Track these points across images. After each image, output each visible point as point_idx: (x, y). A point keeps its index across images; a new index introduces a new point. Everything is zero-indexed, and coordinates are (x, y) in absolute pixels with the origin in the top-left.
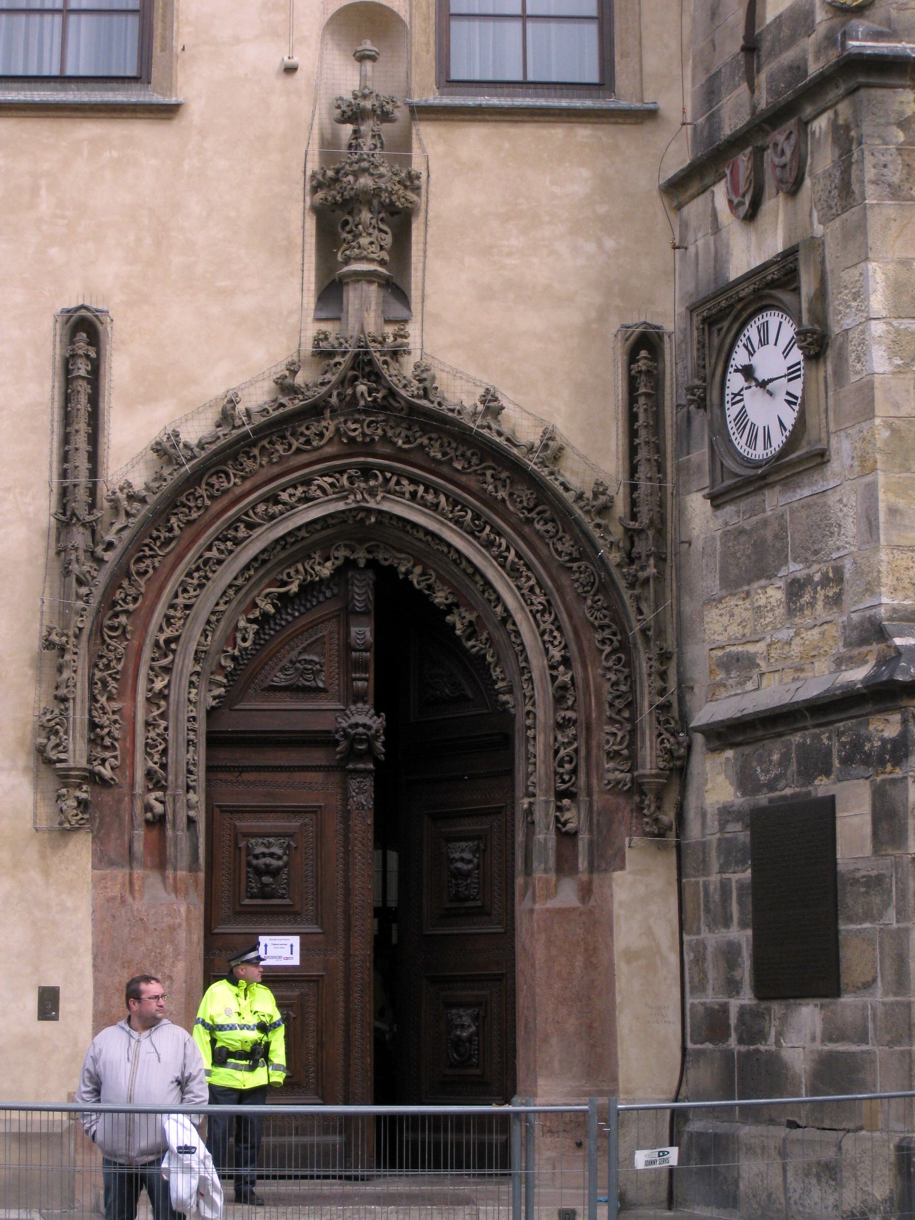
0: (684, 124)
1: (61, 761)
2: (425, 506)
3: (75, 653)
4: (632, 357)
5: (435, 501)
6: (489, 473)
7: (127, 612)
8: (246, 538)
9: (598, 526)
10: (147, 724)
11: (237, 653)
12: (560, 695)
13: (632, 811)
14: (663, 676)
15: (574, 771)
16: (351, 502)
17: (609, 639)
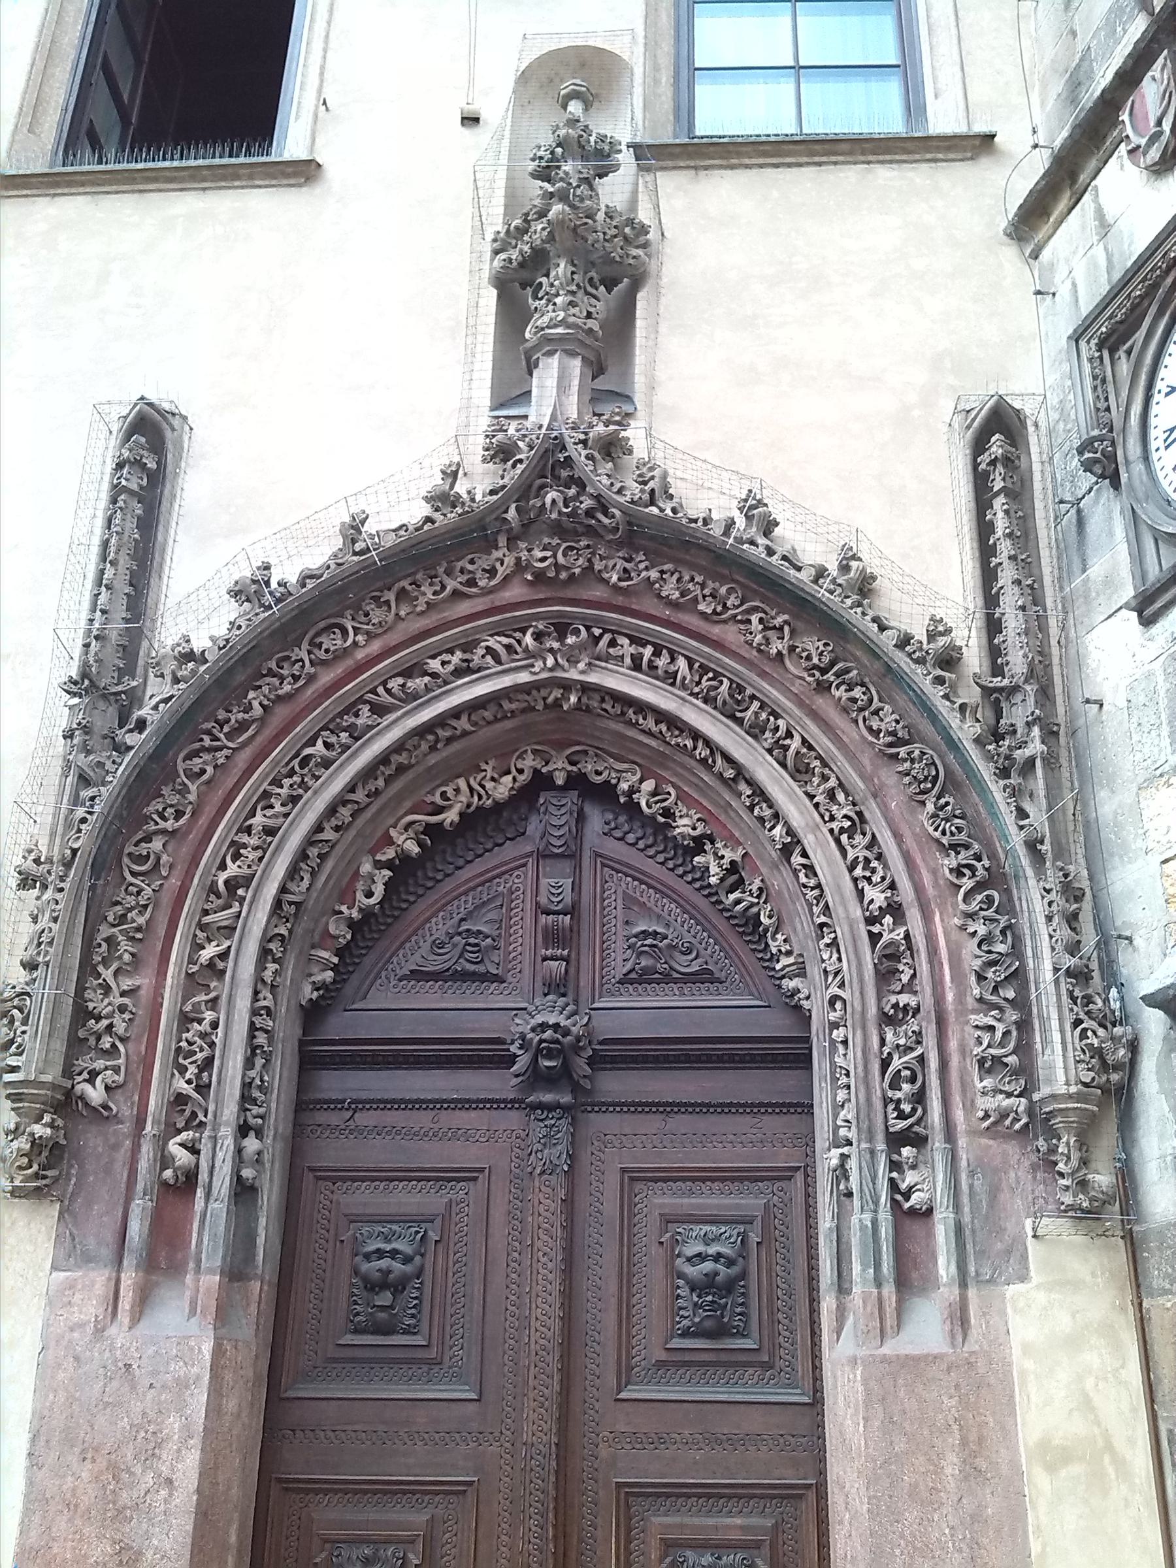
0: (1036, 146)
1: (14, 1069)
2: (657, 678)
3: (61, 890)
4: (979, 445)
5: (672, 668)
6: (755, 618)
7: (164, 832)
8: (370, 727)
9: (939, 680)
10: (186, 1020)
11: (355, 914)
12: (889, 964)
13: (1034, 1168)
14: (1072, 919)
15: (920, 1098)
16: (539, 671)
17: (968, 866)
